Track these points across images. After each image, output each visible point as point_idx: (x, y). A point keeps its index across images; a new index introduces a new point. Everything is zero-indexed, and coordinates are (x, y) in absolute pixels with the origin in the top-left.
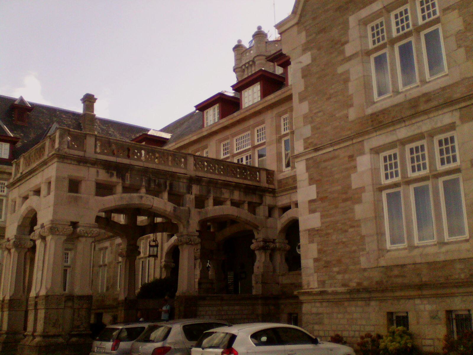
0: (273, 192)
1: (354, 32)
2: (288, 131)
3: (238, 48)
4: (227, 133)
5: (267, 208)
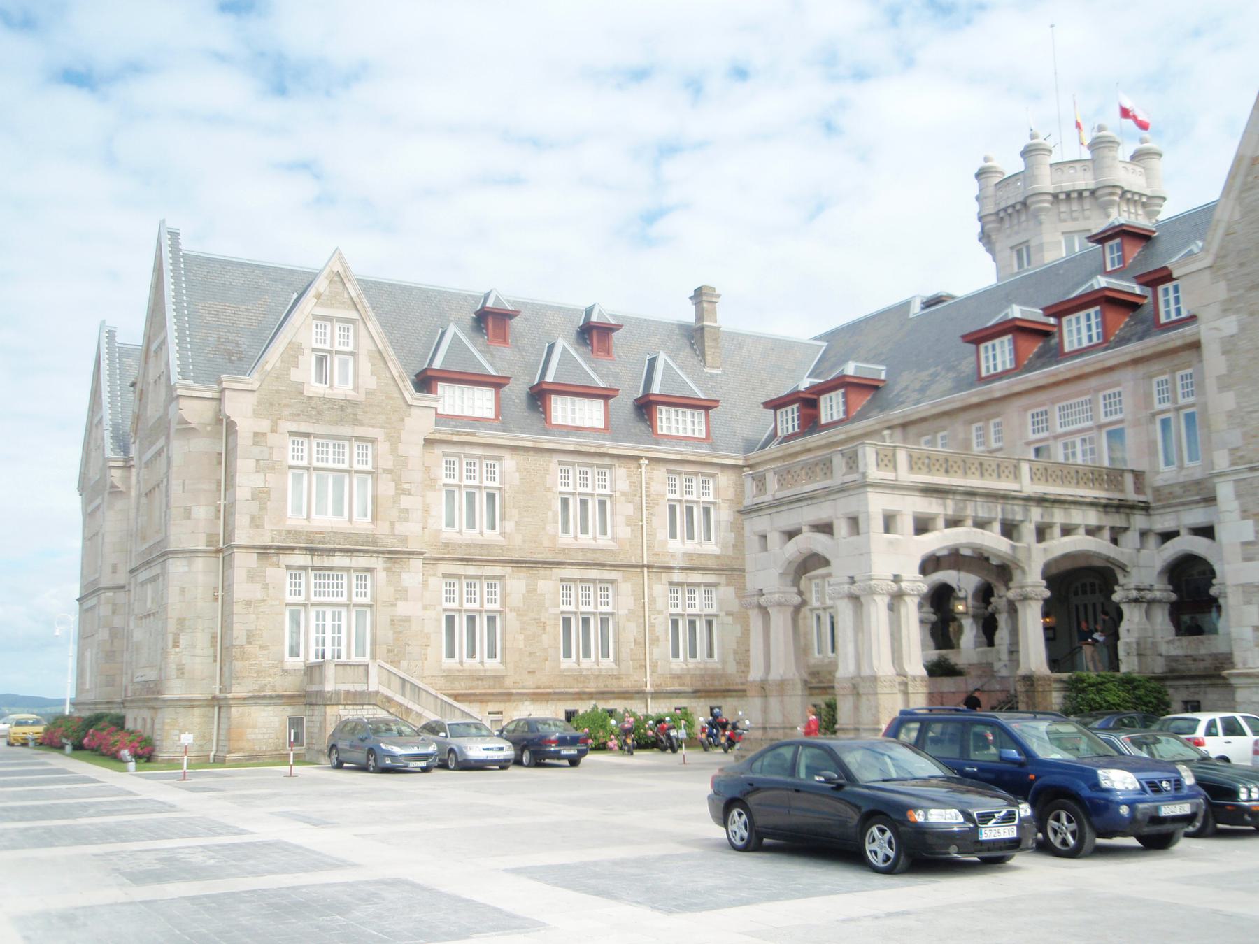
0: (1146, 508)
2: (1166, 405)
4: (1042, 396)
5: (1137, 535)
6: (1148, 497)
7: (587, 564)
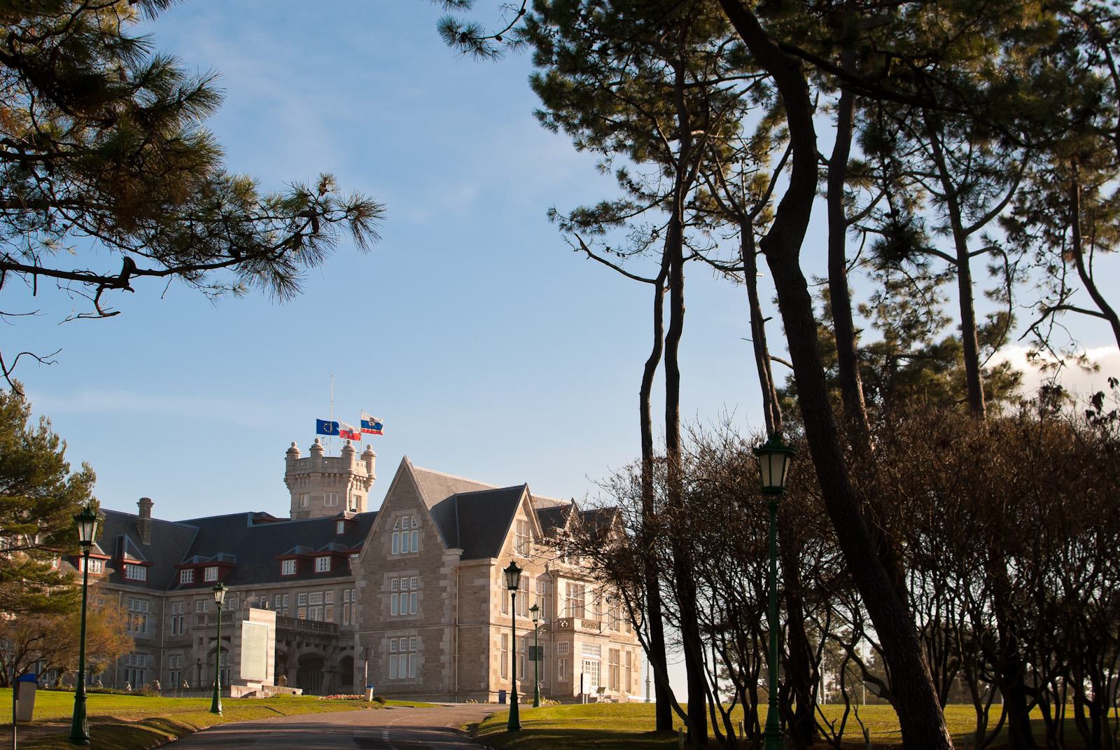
0: (337, 638)
1: (385, 581)
3: (291, 452)
4: (306, 589)
6: (339, 634)
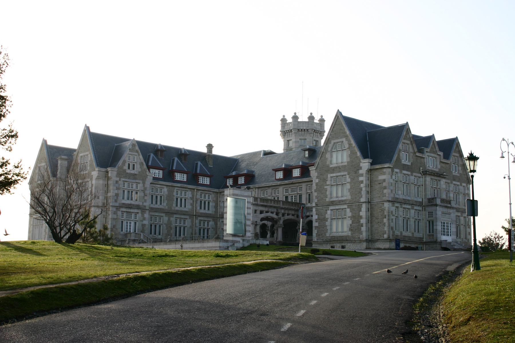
1: (329, 179)
2: (310, 191)
3: (284, 120)
7: (181, 214)
